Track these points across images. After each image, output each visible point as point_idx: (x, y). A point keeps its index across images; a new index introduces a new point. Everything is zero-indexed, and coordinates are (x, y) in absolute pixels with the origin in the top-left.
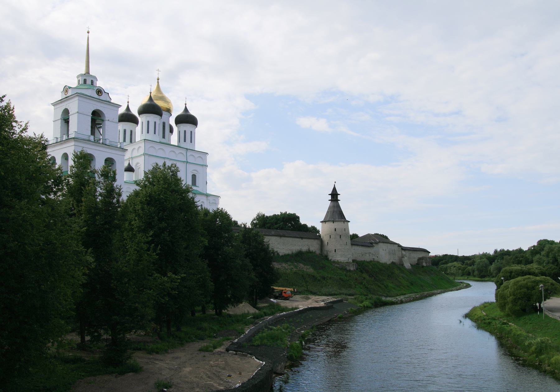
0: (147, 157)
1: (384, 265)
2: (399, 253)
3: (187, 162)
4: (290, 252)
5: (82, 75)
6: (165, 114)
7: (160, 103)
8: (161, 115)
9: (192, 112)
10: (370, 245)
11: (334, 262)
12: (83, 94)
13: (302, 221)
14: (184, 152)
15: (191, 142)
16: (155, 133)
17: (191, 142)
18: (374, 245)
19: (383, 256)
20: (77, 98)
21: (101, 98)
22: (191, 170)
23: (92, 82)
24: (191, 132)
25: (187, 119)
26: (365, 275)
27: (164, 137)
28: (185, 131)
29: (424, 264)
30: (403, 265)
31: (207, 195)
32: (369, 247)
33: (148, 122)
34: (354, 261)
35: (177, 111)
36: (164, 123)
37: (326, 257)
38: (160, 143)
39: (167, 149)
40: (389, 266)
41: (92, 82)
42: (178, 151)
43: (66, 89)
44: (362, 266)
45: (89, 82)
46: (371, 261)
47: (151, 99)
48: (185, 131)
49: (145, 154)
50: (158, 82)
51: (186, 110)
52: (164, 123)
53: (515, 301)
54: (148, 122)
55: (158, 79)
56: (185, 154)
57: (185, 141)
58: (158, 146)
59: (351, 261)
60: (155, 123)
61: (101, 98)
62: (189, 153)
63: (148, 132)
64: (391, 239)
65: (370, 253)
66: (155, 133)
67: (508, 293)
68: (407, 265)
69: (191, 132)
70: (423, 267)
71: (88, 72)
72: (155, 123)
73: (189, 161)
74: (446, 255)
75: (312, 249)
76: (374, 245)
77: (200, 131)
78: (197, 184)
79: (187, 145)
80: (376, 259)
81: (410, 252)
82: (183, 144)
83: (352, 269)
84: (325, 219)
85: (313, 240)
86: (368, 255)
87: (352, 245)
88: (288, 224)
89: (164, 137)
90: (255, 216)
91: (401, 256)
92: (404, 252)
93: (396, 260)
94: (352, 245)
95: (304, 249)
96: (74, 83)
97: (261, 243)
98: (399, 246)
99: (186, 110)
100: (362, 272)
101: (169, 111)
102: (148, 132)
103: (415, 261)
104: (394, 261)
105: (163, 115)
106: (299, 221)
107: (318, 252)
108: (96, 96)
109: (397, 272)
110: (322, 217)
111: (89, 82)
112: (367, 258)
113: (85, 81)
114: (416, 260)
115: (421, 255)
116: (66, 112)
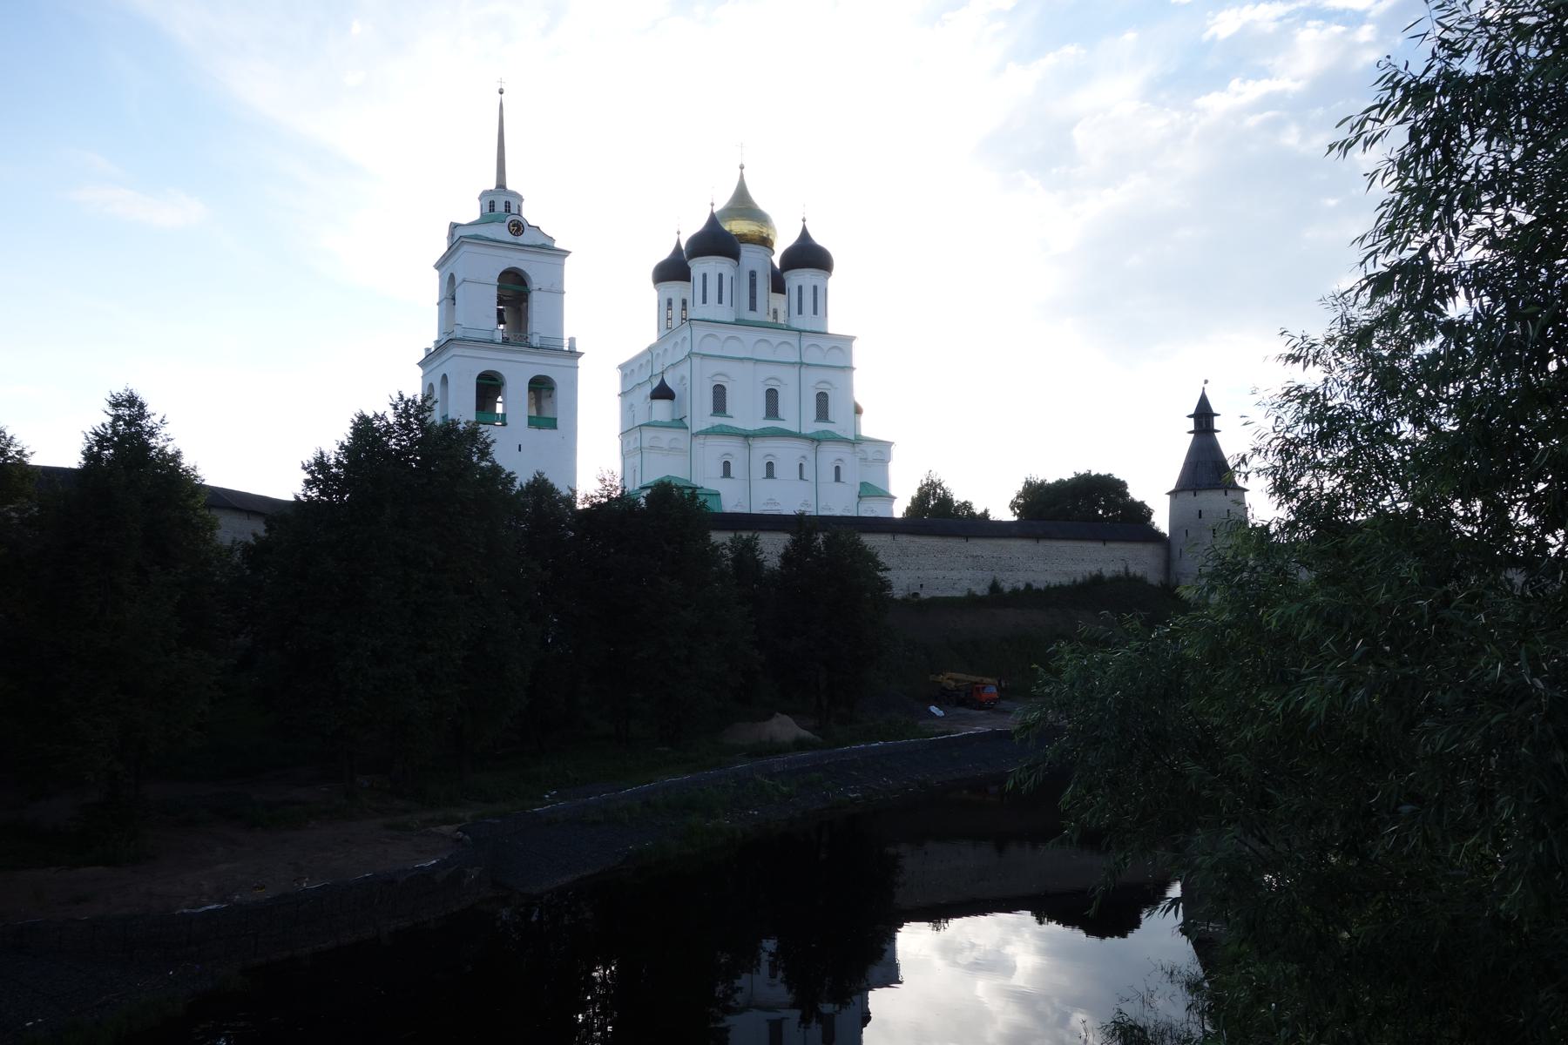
0: (696, 361)
3: (801, 364)
4: (1065, 581)
5: (485, 194)
6: (746, 251)
7: (736, 227)
8: (734, 255)
9: (819, 238)
12: (488, 239)
14: (792, 338)
15: (815, 312)
16: (720, 301)
17: (815, 312)
20: (465, 248)
21: (522, 239)
22: (812, 379)
23: (508, 205)
24: (815, 288)
25: (809, 256)
28: (800, 288)
31: (858, 441)
33: (705, 276)
35: (784, 241)
38: (739, 322)
41: (508, 205)
42: (776, 337)
43: (454, 227)
45: (500, 207)
47: (713, 221)
48: (800, 288)
49: (689, 356)
50: (742, 176)
51: (805, 235)
54: (705, 276)
55: (742, 167)
57: (800, 312)
58: (723, 333)
60: (721, 276)
61: (522, 239)
62: (807, 341)
63: (704, 302)
66: (720, 301)
69: (815, 288)
71: (501, 185)
72: (721, 276)
73: (805, 360)
75: (1136, 569)
77: (837, 285)
78: (831, 417)
82: (797, 322)
84: (1179, 483)
85: (1138, 546)
90: (1020, 488)
95: (1109, 570)
96: (470, 212)
99: (805, 235)
102: (704, 302)
108: (510, 238)
110: (1171, 480)
111: (500, 207)
113: (492, 205)
116: (452, 277)
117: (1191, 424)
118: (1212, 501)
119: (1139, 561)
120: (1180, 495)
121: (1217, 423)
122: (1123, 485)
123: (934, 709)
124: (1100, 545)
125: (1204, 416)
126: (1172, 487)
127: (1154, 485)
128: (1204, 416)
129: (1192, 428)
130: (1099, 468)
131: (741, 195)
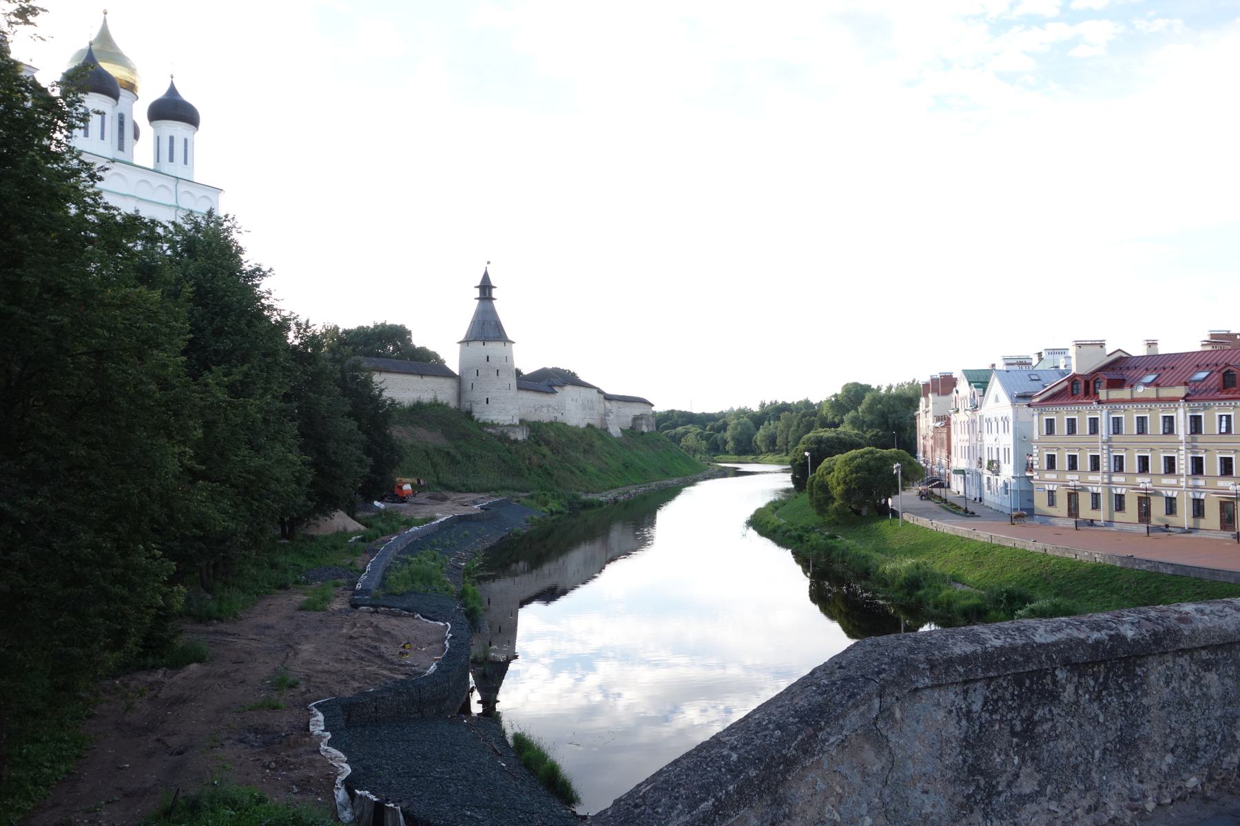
1: (574, 429)
2: (602, 406)
6: (123, 93)
8: (116, 97)
9: (186, 95)
10: (548, 389)
11: (485, 424)
13: (418, 341)
14: (171, 184)
15: (186, 163)
16: (102, 138)
17: (186, 163)
18: (556, 389)
19: (571, 410)
24: (186, 140)
25: (173, 109)
26: (545, 450)
27: (121, 148)
28: (172, 138)
29: (645, 429)
30: (606, 430)
32: (547, 393)
34: (521, 421)
35: (150, 91)
36: (121, 118)
37: (469, 414)
39: (133, 176)
40: (584, 431)
42: (156, 180)
44: (542, 434)
46: (551, 423)
48: (172, 138)
50: (105, 21)
51: (172, 91)
52: (121, 118)
53: (847, 494)
56: (172, 187)
57: (171, 160)
59: (516, 421)
62: (183, 187)
64: (583, 377)
65: (549, 406)
66: (102, 138)
67: (834, 480)
68: (615, 431)
69: (186, 140)
70: (643, 433)
74: (673, 411)
75: (442, 398)
76: (556, 389)
77: (202, 139)
79: (177, 169)
80: (560, 419)
81: (620, 404)
82: (166, 167)
83: (520, 438)
85: (442, 380)
86: (545, 410)
87: (519, 388)
88: (388, 345)
89: (121, 148)
91: (602, 411)
92: (608, 404)
93: (596, 422)
94: (519, 388)
95: (426, 398)
97: (367, 383)
98: (600, 392)
99: (172, 91)
100: (537, 443)
101: (131, 87)
103: (627, 422)
104: (591, 422)
105: (121, 98)
106: (410, 340)
107: (453, 405)
109: (598, 443)
110: (462, 332)
112: (545, 416)
114: (630, 419)
115: (638, 410)
117: (477, 293)
118: (493, 348)
119: (442, 392)
120: (471, 344)
121: (495, 293)
122: (410, 333)
123: (377, 503)
124: (417, 378)
125: (486, 288)
126: (462, 338)
127: (441, 333)
128: (486, 288)
129: (478, 295)
130: (392, 320)
131: (104, 36)
